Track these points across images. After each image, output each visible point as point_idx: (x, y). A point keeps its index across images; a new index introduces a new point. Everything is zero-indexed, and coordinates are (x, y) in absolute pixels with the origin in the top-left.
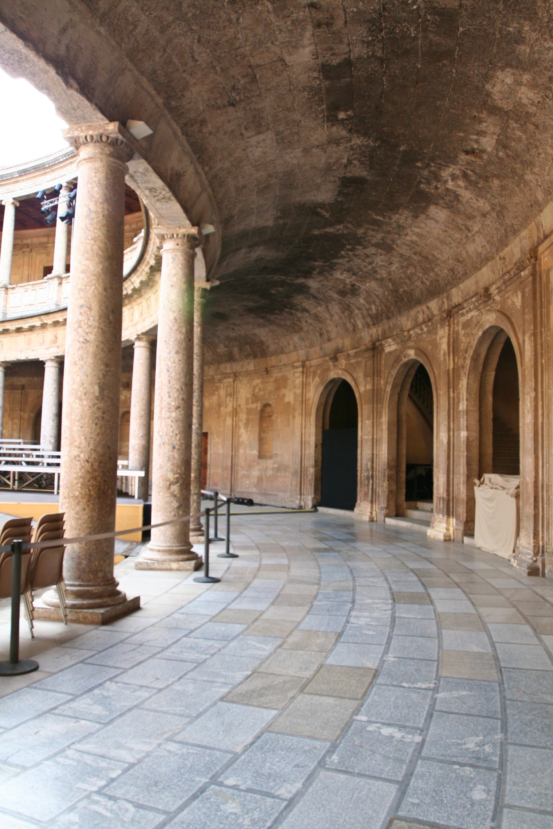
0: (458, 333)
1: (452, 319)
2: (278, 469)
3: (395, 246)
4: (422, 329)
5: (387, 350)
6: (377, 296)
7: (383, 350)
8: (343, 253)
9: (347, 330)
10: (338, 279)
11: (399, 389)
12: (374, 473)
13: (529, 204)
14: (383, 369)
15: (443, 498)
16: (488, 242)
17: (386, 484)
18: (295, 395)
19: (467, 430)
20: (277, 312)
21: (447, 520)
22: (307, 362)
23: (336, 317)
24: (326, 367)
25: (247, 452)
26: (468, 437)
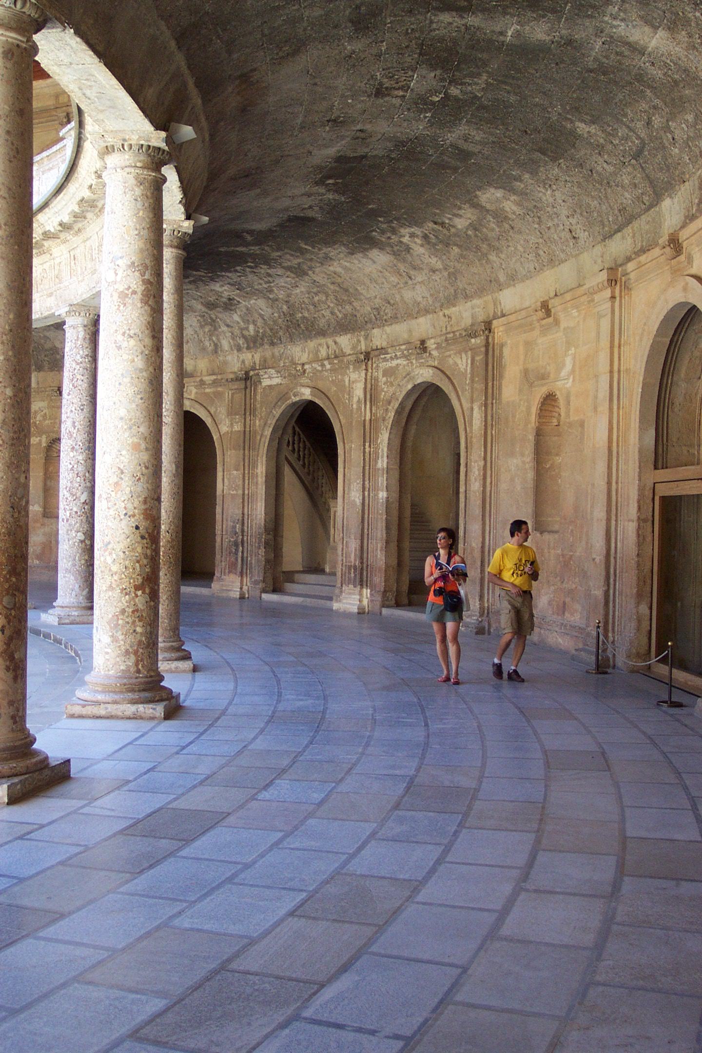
0: (377, 379)
1: (370, 362)
3: (310, 272)
4: (323, 365)
5: (266, 382)
6: (261, 316)
7: (260, 382)
8: (238, 268)
9: (204, 349)
11: (280, 432)
12: (245, 539)
13: (488, 279)
14: (258, 406)
15: (355, 567)
16: (431, 295)
17: (262, 551)
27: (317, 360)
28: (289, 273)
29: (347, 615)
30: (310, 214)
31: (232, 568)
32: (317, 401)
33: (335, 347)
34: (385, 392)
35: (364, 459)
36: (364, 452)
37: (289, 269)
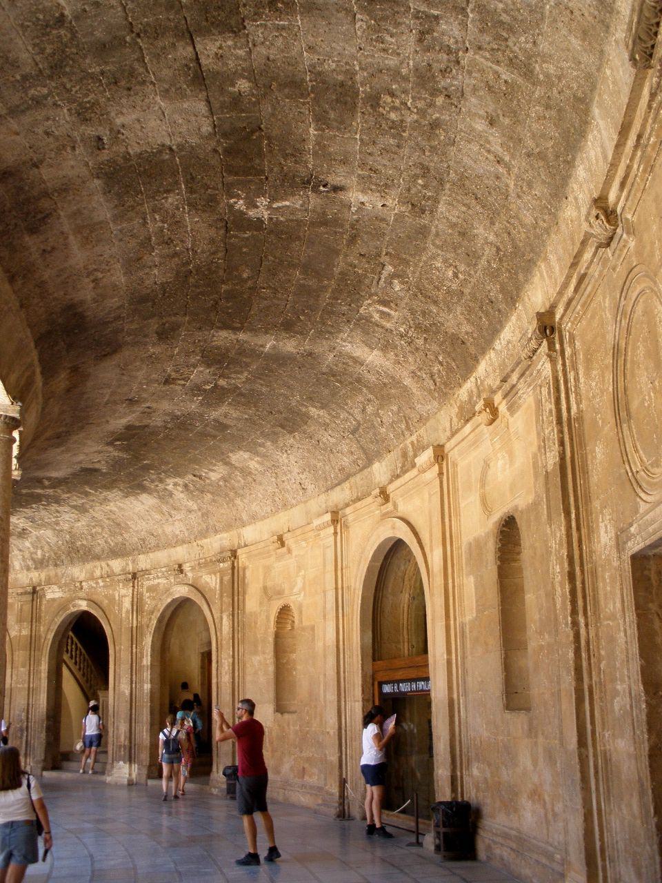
0: (142, 594)
1: (136, 581)
4: (97, 583)
5: (49, 596)
6: (48, 543)
8: (34, 506)
14: (43, 615)
17: (43, 735)
27: (92, 578)
28: (73, 510)
29: (117, 786)
30: (97, 466)
33: (107, 569)
35: (132, 659)
36: (132, 653)
37: (74, 507)
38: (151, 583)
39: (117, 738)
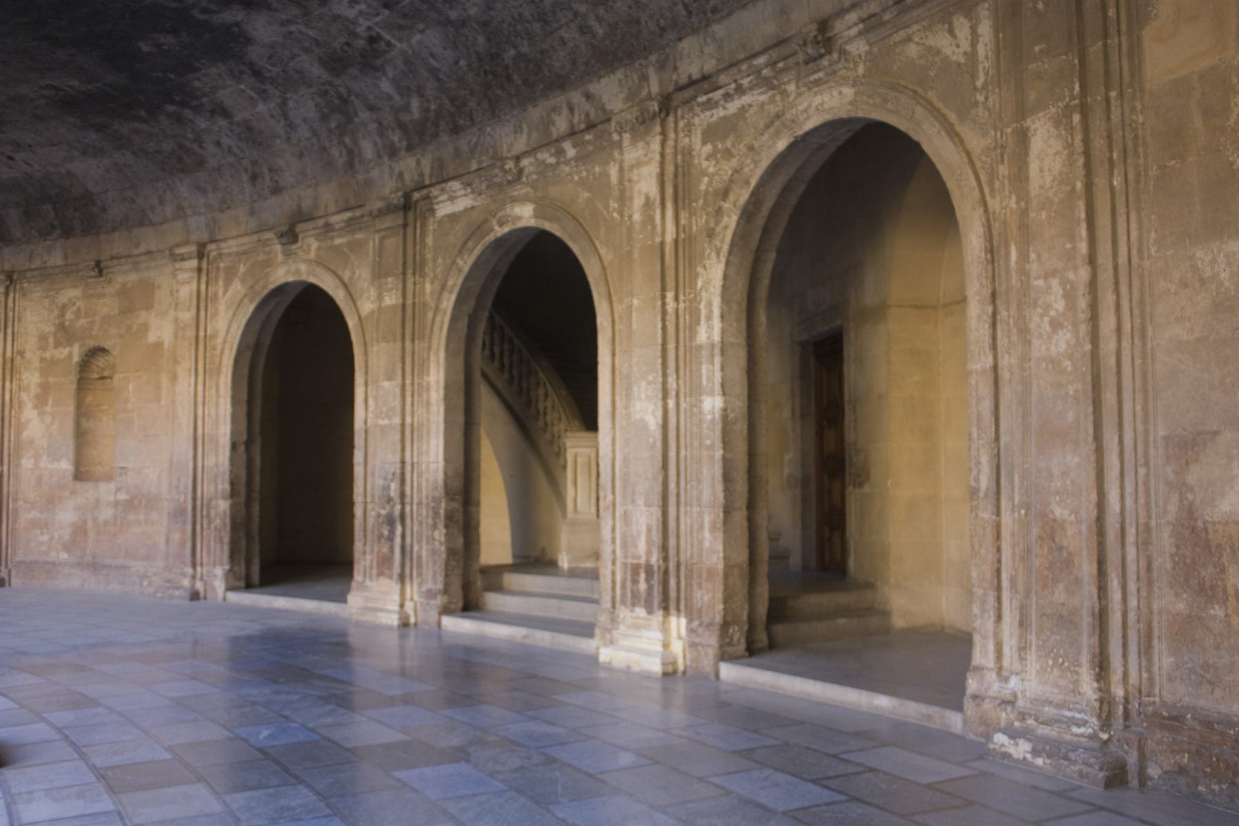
0: (688, 153)
1: (671, 119)
2: (130, 505)
4: (560, 152)
5: (444, 209)
6: (434, 72)
7: (432, 211)
10: (336, 18)
12: (408, 509)
14: (429, 256)
15: (649, 569)
17: (440, 534)
18: (178, 326)
19: (724, 394)
20: (143, 113)
21: (664, 623)
22: (212, 247)
23: (303, 132)
24: (262, 257)
25: (44, 463)
26: (725, 410)
29: (633, 679)
31: (384, 563)
32: (548, 226)
34: (711, 176)
35: (664, 328)
36: (664, 313)
38: (720, 113)
39: (624, 545)
